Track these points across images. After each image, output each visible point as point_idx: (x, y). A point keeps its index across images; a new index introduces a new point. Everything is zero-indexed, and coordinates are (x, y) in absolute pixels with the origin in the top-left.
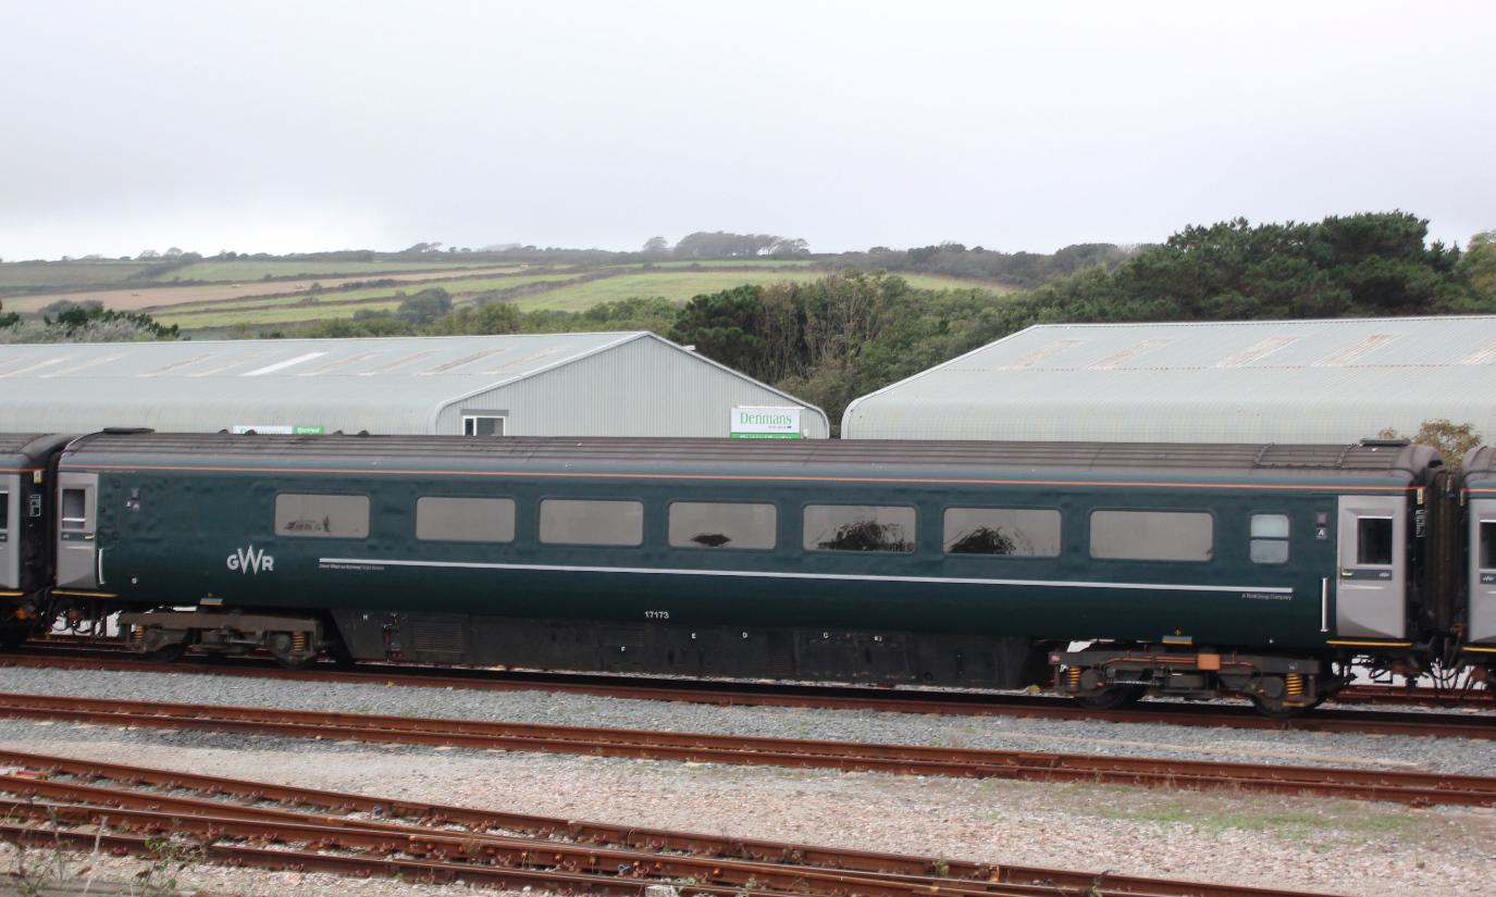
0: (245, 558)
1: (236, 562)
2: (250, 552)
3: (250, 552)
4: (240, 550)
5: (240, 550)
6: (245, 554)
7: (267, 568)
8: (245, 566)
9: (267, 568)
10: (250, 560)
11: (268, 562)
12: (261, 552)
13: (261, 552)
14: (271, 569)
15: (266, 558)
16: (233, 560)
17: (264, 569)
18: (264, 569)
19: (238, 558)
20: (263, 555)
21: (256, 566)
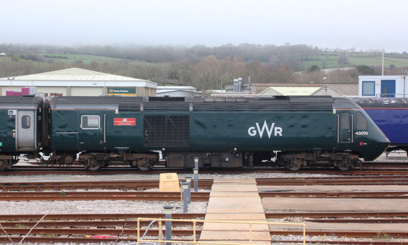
0: (261, 130)
1: (255, 132)
2: (265, 125)
3: (265, 125)
4: (257, 124)
5: (257, 124)
6: (261, 126)
7: (278, 134)
8: (261, 134)
9: (278, 134)
10: (265, 129)
11: (279, 131)
12: (273, 124)
13: (273, 124)
14: (281, 135)
15: (276, 128)
16: (253, 130)
17: (276, 135)
18: (276, 135)
19: (256, 129)
20: (275, 126)
21: (269, 134)
